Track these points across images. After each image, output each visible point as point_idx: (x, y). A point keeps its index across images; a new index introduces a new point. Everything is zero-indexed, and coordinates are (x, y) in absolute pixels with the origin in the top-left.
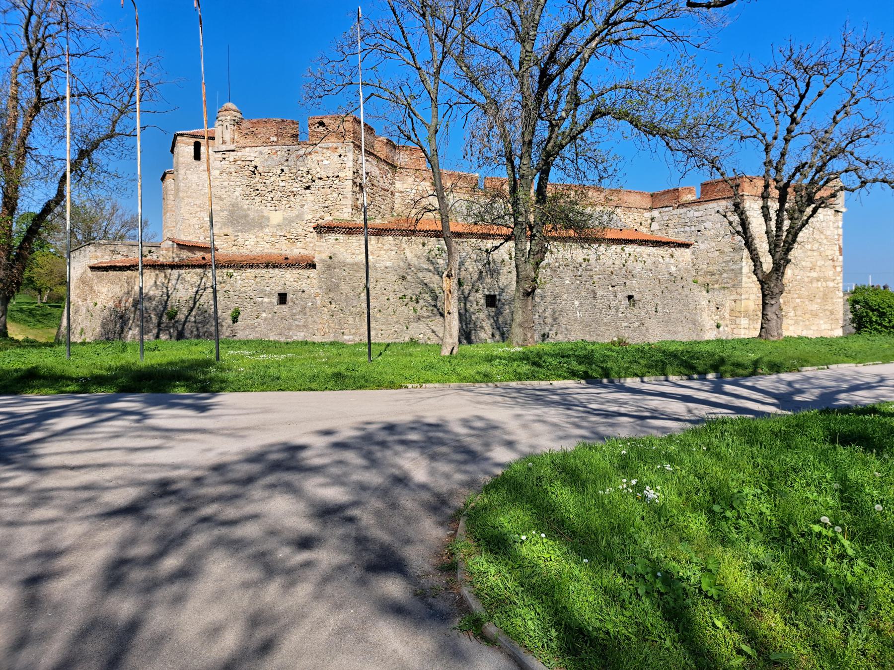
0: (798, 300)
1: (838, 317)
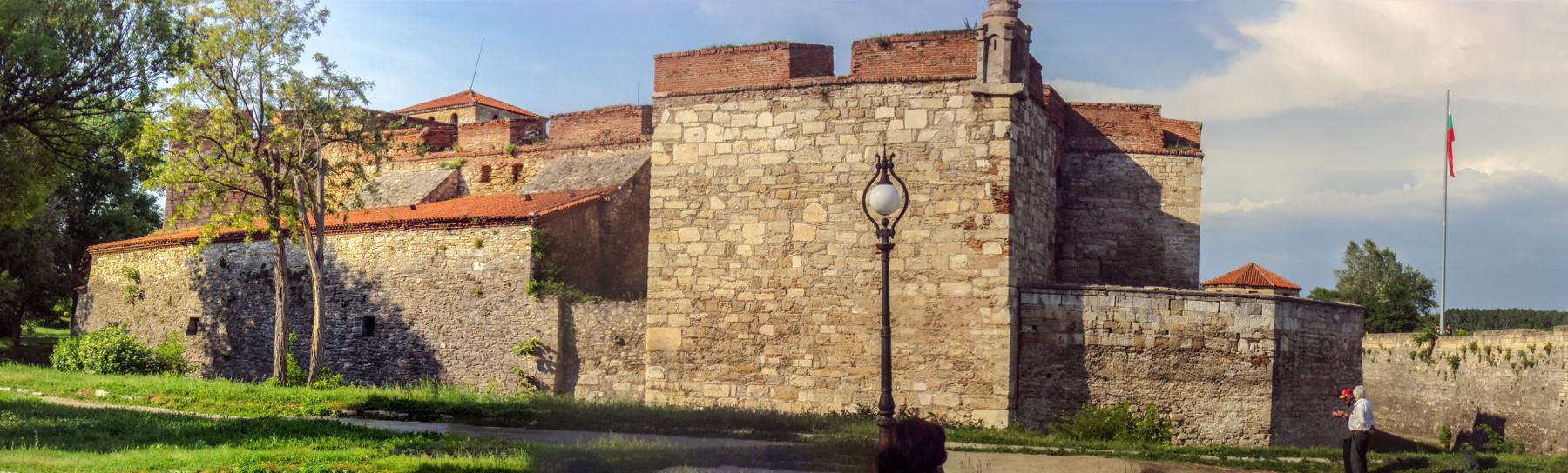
0: (825, 329)
1: (987, 376)
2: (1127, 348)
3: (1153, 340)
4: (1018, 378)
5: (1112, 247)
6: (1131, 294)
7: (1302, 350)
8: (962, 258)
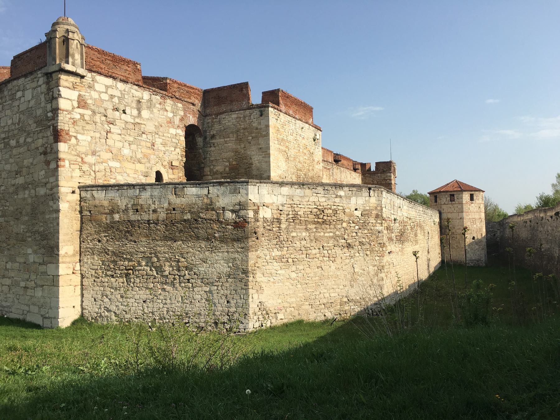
2: (148, 221)
3: (165, 215)
4: (80, 244)
5: (226, 167)
6: (149, 187)
7: (291, 216)
8: (43, 172)
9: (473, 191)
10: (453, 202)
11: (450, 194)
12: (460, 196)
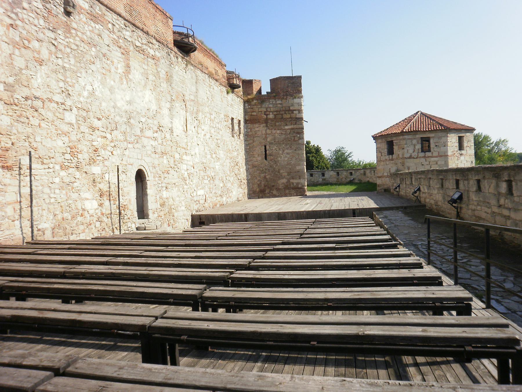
9: (471, 130)
10: (428, 154)
11: (421, 138)
12: (443, 140)
